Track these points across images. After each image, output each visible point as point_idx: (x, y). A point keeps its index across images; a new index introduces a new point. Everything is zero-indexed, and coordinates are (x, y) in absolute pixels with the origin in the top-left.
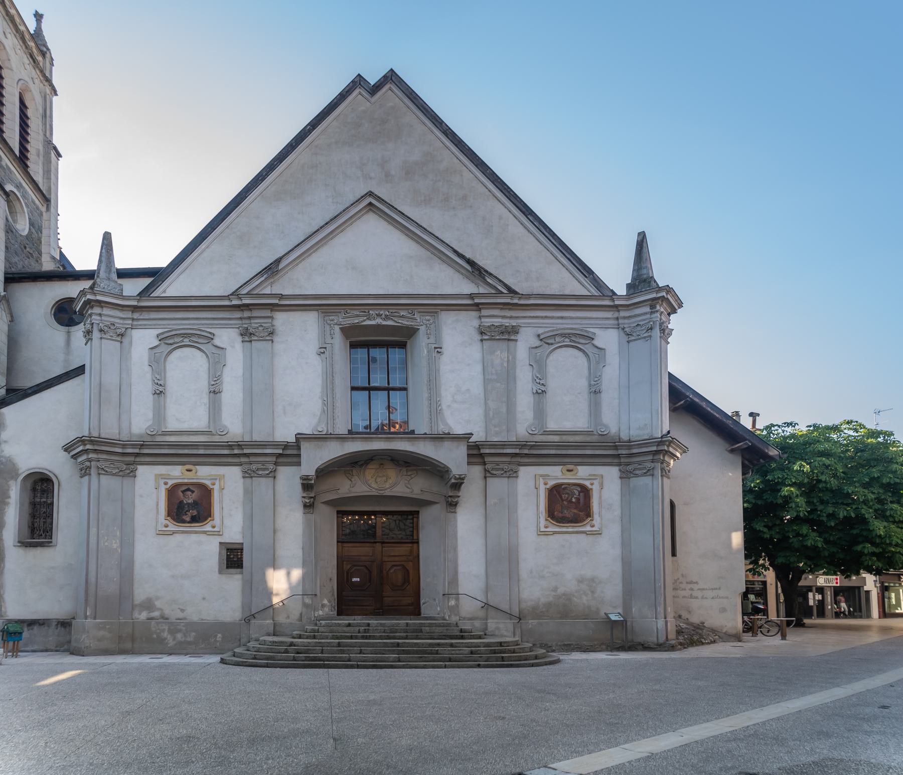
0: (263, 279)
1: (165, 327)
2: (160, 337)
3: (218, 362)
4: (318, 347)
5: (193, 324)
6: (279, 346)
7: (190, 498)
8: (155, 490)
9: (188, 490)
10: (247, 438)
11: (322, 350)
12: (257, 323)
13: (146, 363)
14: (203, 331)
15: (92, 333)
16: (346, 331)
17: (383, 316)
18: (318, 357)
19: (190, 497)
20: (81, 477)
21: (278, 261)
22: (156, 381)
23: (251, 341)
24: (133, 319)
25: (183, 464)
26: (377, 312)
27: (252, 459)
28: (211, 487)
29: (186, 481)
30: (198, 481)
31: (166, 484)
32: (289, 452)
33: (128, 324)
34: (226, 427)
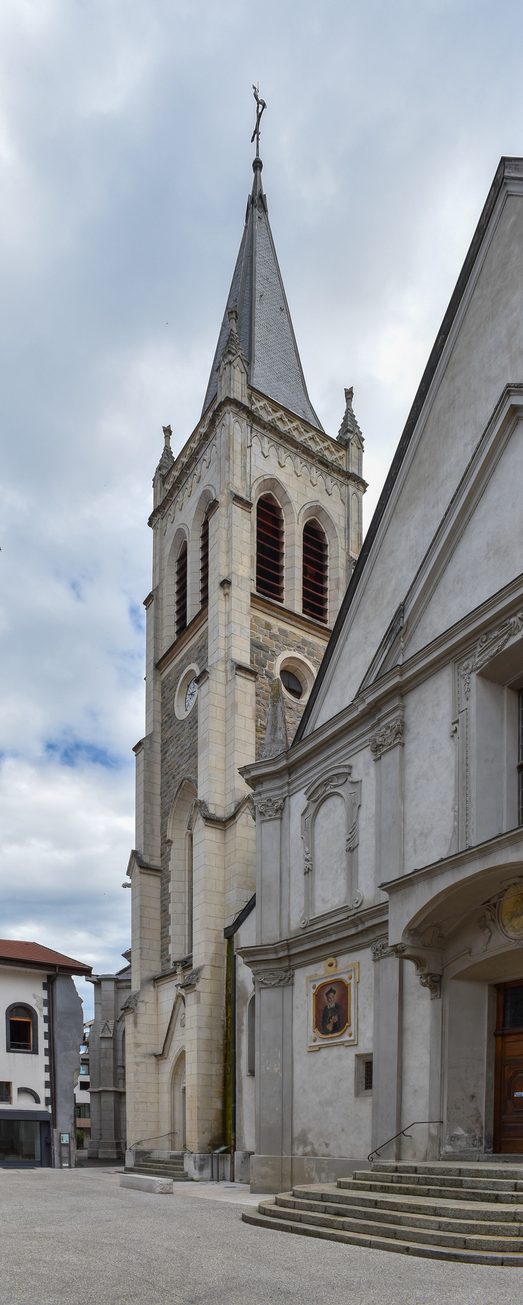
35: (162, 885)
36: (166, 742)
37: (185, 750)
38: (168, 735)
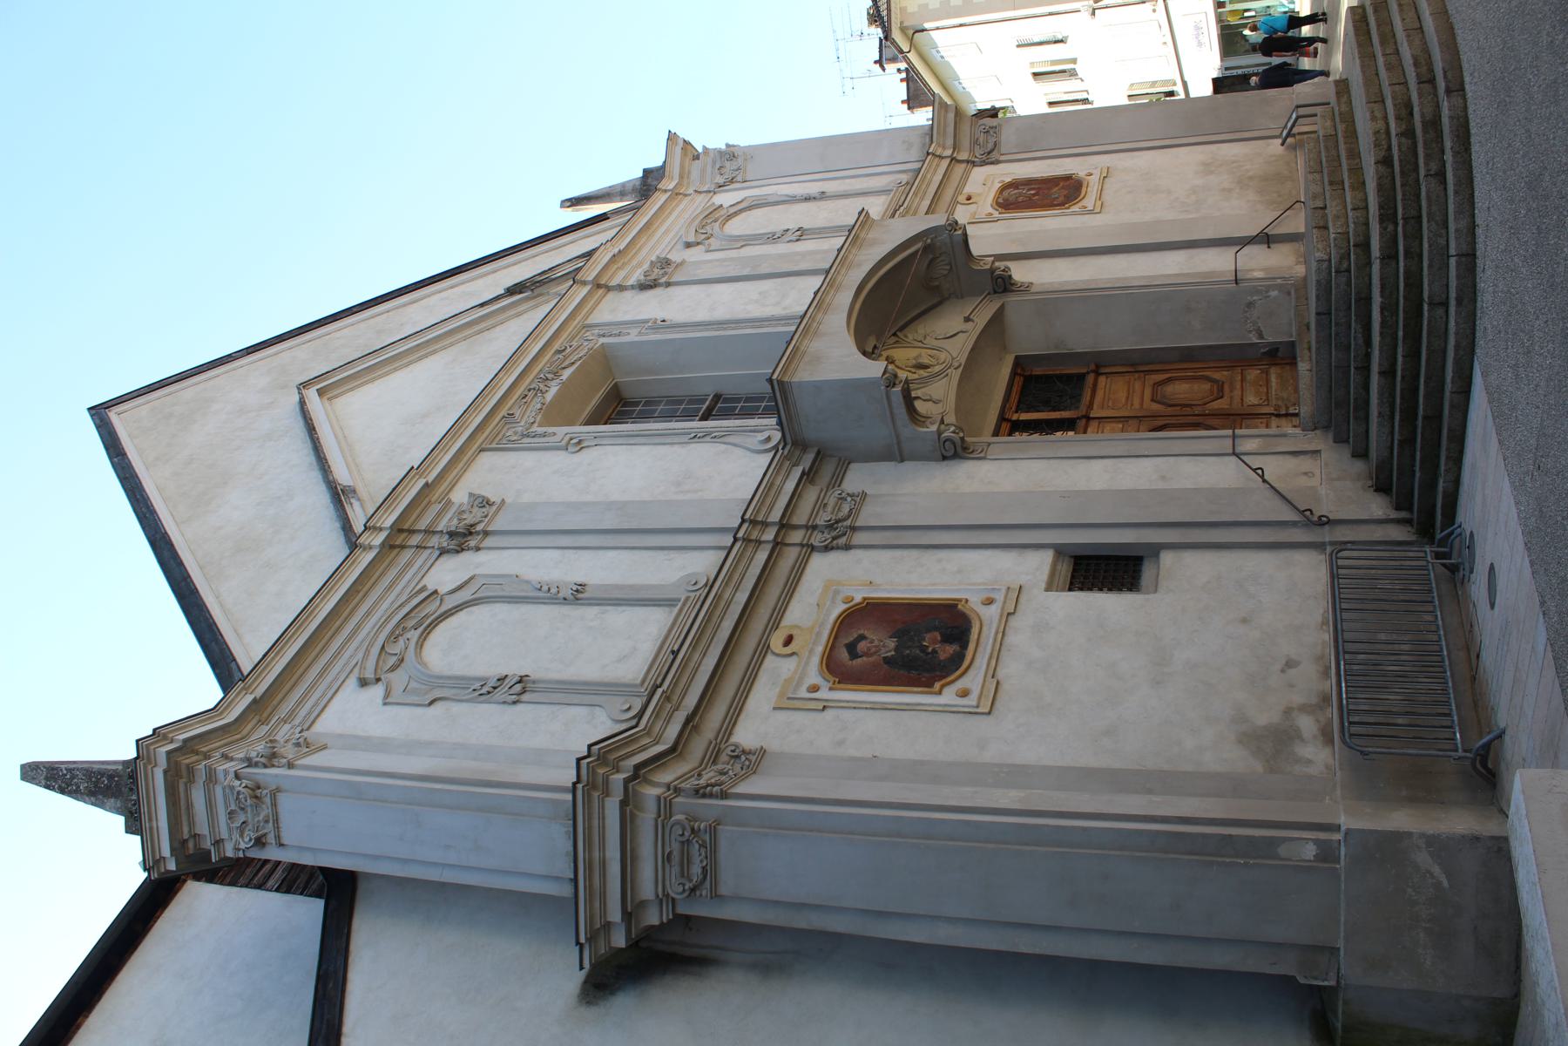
1: (348, 670)
8: (829, 714)
19: (876, 643)
25: (763, 649)
30: (829, 627)
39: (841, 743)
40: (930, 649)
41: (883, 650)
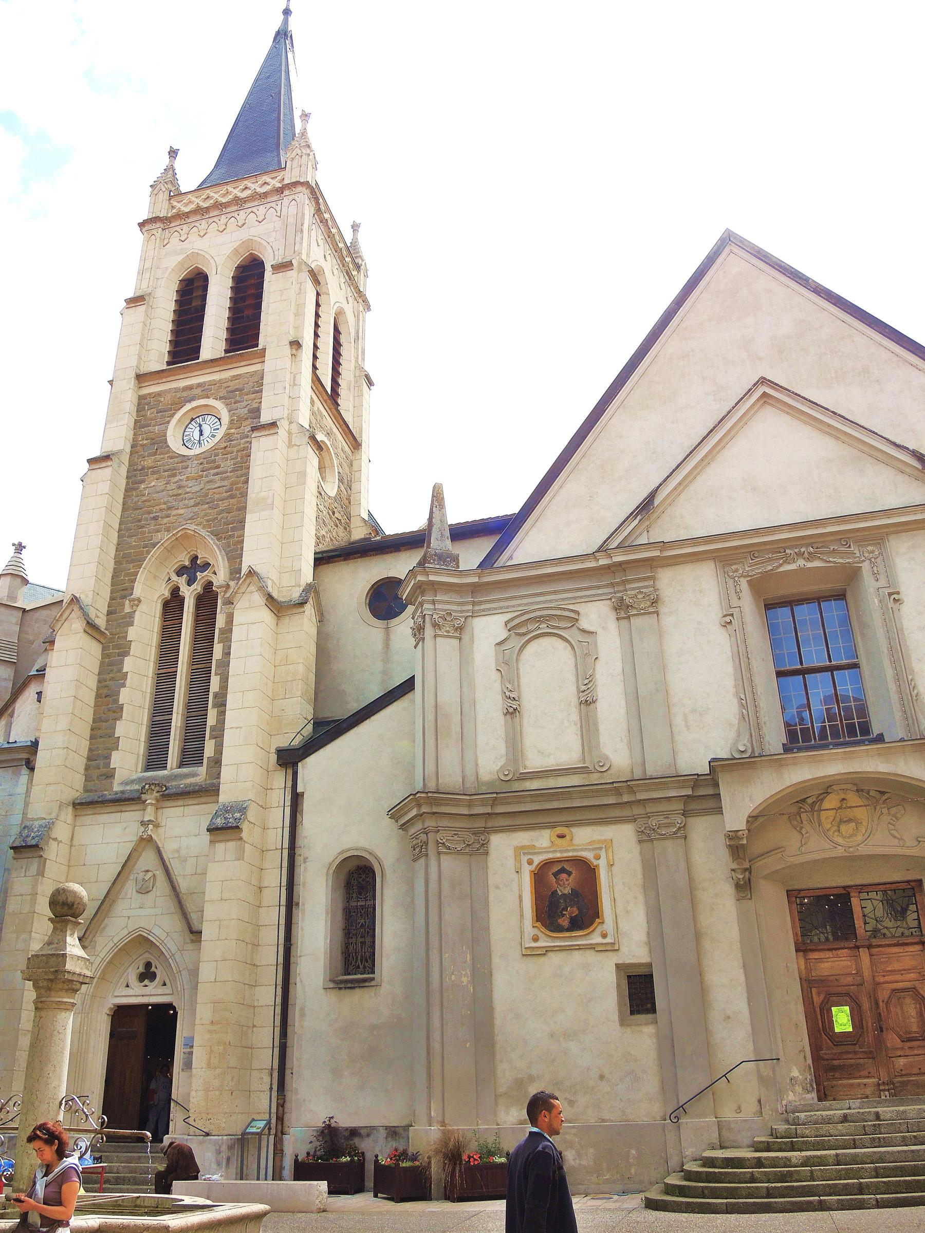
0: (636, 522)
2: (509, 626)
3: (587, 655)
4: (721, 615)
5: (551, 601)
6: (668, 620)
7: (565, 887)
8: (517, 874)
9: (563, 870)
10: (638, 774)
11: (728, 619)
12: (634, 589)
13: (493, 668)
14: (564, 609)
15: (424, 629)
16: (756, 586)
17: (806, 555)
18: (723, 630)
20: (414, 860)
21: (652, 496)
22: (508, 694)
23: (629, 618)
24: (474, 604)
25: (553, 826)
26: (796, 550)
27: (650, 808)
28: (595, 862)
29: (558, 855)
30: (575, 854)
31: (530, 862)
32: (701, 792)
33: (468, 611)
34: (607, 758)
35: (104, 655)
36: (141, 470)
37: (187, 493)
38: (149, 462)
39: (497, 887)
40: (565, 913)
41: (562, 888)
